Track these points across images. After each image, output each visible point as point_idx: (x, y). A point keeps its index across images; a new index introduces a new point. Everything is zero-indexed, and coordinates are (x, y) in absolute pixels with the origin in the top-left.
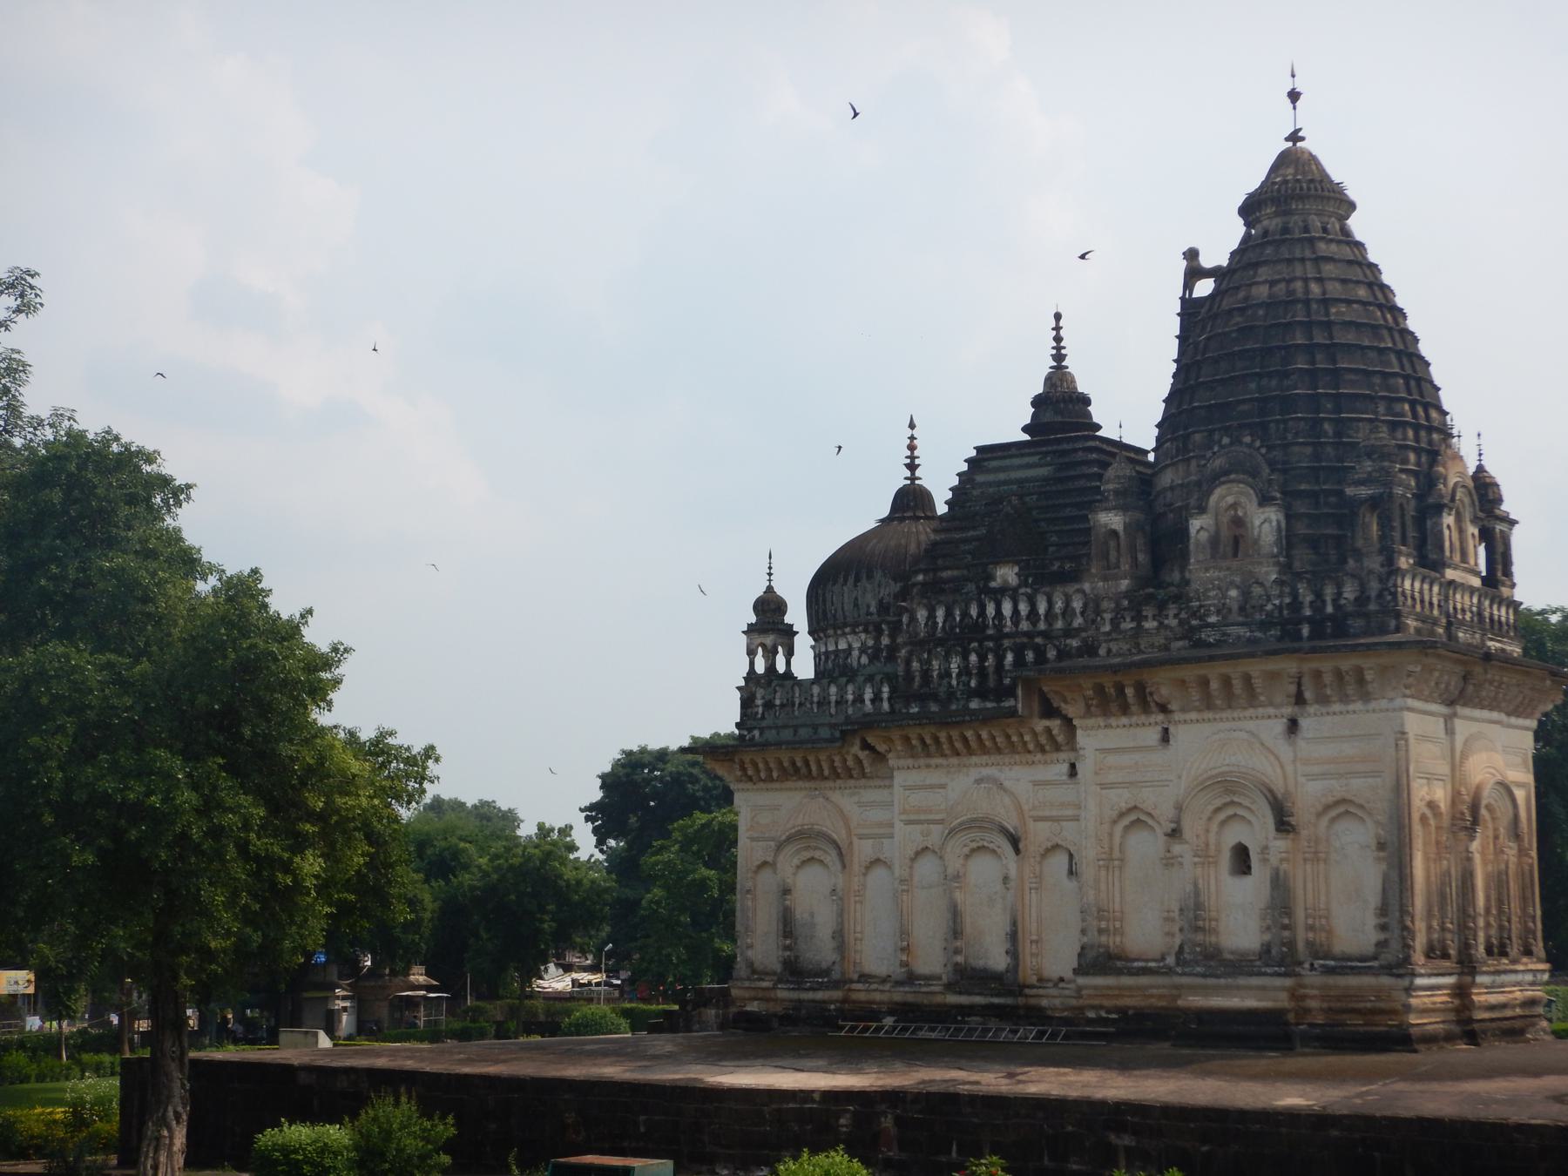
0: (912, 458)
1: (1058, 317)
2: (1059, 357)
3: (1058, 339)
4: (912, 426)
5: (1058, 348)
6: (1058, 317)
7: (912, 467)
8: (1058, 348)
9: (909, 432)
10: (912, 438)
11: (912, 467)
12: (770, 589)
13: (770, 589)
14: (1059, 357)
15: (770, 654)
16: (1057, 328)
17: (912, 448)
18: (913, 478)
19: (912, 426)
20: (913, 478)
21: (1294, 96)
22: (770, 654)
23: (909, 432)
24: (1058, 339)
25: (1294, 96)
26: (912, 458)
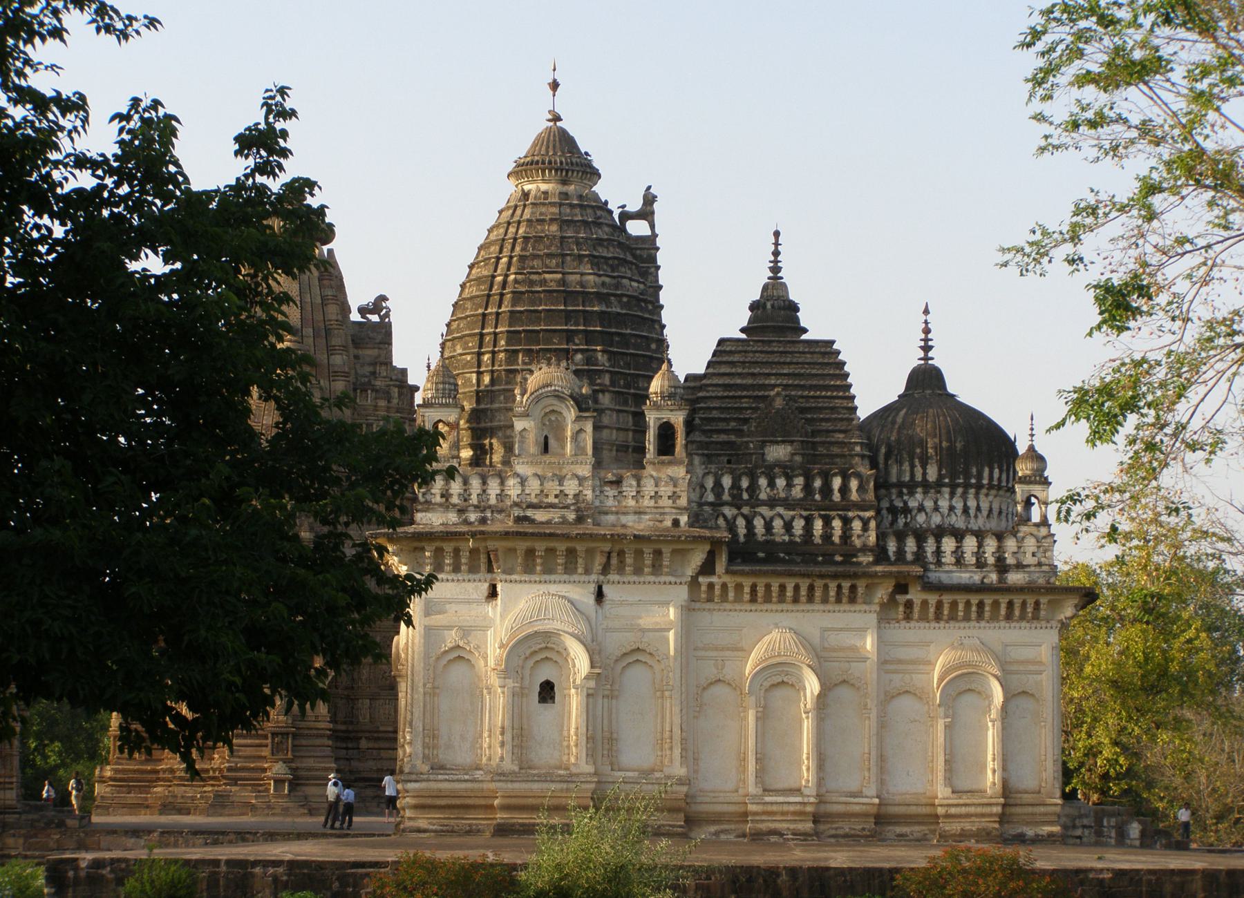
0: (926, 340)
1: (777, 234)
2: (775, 269)
3: (776, 253)
4: (926, 312)
5: (776, 262)
6: (777, 234)
7: (927, 348)
9: (929, 318)
10: (926, 322)
11: (927, 348)
14: (775, 269)
16: (777, 244)
17: (927, 331)
18: (926, 358)
19: (926, 312)
20: (926, 358)
21: (555, 86)
23: (929, 318)
24: (776, 253)
25: (555, 86)
26: (926, 340)
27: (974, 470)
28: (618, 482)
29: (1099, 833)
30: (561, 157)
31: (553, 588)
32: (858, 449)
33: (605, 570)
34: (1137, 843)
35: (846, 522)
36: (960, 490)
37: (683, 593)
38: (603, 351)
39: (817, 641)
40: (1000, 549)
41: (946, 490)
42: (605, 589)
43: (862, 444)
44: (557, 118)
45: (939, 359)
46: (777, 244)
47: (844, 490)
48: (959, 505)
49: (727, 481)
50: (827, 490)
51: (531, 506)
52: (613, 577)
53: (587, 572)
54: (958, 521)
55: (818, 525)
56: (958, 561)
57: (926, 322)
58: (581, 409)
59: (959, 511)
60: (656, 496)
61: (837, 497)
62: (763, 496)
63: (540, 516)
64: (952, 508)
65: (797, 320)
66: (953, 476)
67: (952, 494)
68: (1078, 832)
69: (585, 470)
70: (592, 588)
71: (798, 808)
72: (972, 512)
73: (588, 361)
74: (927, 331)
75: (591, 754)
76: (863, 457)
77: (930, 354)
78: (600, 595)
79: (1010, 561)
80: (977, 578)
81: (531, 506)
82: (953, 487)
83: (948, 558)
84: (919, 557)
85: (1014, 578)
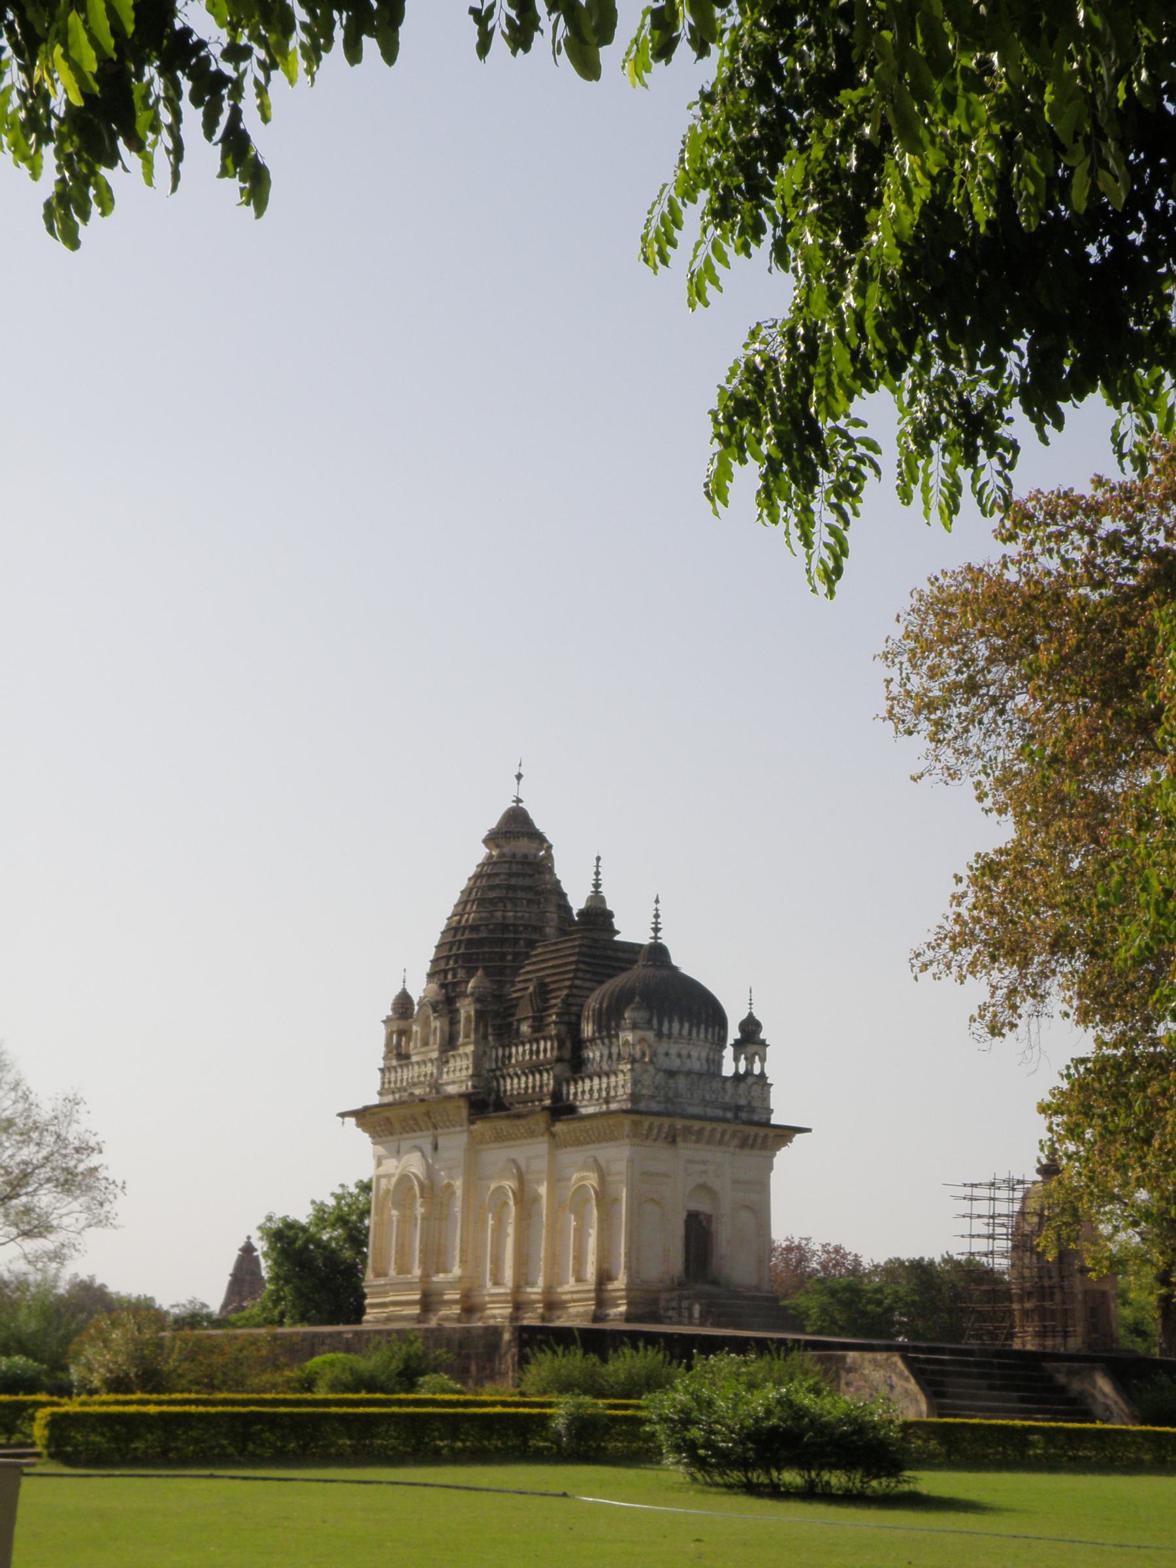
0: (656, 923)
1: (598, 859)
2: (597, 885)
3: (597, 873)
4: (657, 901)
5: (597, 880)
6: (598, 859)
7: (656, 930)
8: (597, 880)
9: (659, 906)
10: (657, 910)
11: (656, 930)
12: (751, 1015)
13: (751, 1015)
14: (597, 885)
15: (750, 1061)
16: (597, 866)
17: (657, 916)
18: (656, 938)
19: (657, 901)
20: (656, 938)
21: (519, 777)
22: (750, 1061)
23: (659, 906)
24: (597, 873)
25: (519, 777)
26: (656, 923)
27: (613, 1024)
28: (447, 1062)
29: (680, 1315)
30: (516, 828)
31: (417, 1142)
32: (554, 1017)
33: (435, 1127)
34: (697, 1321)
35: (541, 1075)
36: (606, 1041)
37: (464, 1138)
38: (463, 967)
39: (523, 1168)
40: (608, 1084)
41: (599, 1041)
42: (441, 1141)
43: (557, 1014)
44: (519, 801)
45: (665, 940)
46: (597, 866)
47: (545, 1051)
48: (606, 1053)
49: (500, 1052)
50: (538, 1052)
51: (414, 1084)
52: (440, 1131)
53: (428, 1129)
54: (605, 1067)
55: (531, 1078)
56: (587, 1095)
57: (657, 910)
58: (435, 1011)
59: (605, 1058)
60: (461, 1070)
61: (542, 1056)
62: (513, 1061)
63: (417, 1092)
64: (601, 1056)
65: (611, 924)
66: (600, 1032)
67: (603, 1044)
68: (670, 1313)
69: (435, 1055)
70: (430, 1139)
71: (502, 1298)
72: (615, 1057)
73: (454, 976)
74: (657, 916)
75: (423, 1263)
76: (555, 1023)
77: (659, 935)
78: (436, 1148)
79: (612, 1093)
80: (597, 1109)
81: (414, 1084)
82: (602, 1039)
83: (587, 1096)
84: (576, 1094)
85: (614, 1106)
